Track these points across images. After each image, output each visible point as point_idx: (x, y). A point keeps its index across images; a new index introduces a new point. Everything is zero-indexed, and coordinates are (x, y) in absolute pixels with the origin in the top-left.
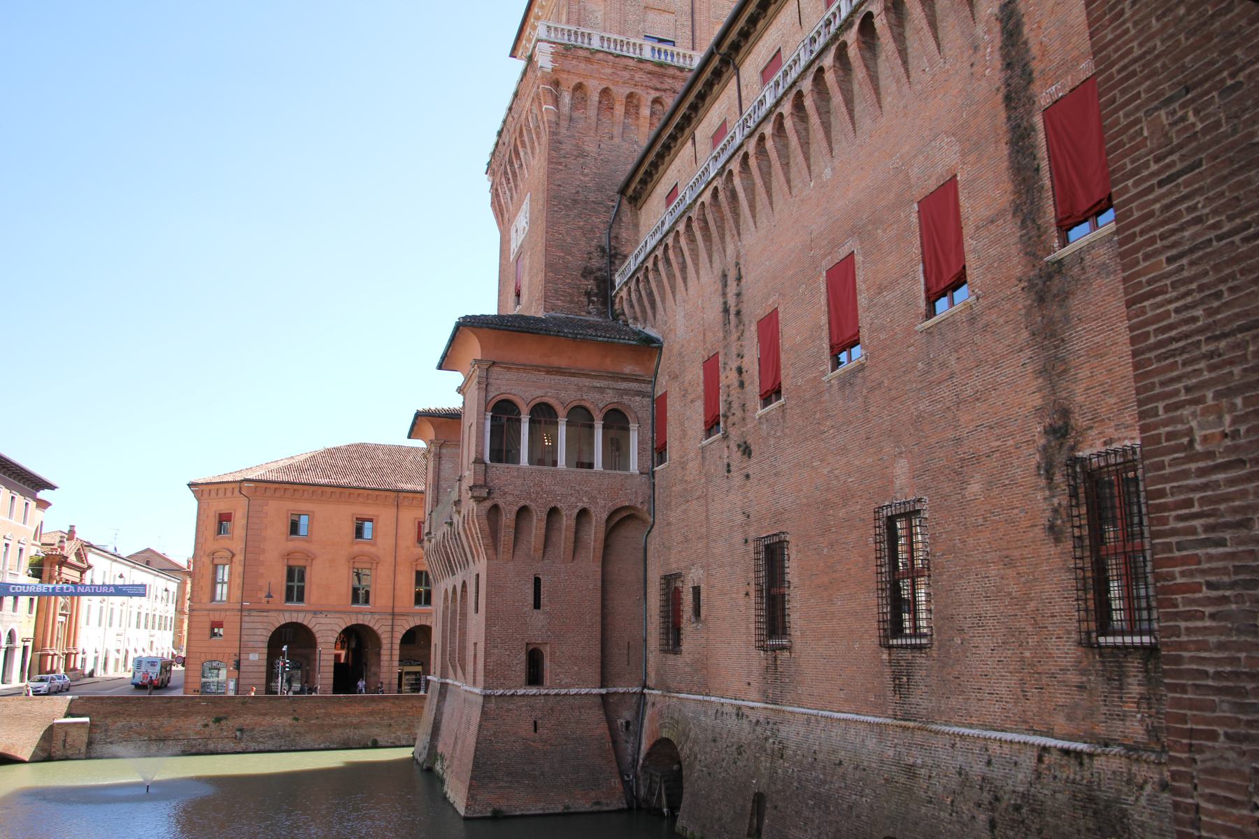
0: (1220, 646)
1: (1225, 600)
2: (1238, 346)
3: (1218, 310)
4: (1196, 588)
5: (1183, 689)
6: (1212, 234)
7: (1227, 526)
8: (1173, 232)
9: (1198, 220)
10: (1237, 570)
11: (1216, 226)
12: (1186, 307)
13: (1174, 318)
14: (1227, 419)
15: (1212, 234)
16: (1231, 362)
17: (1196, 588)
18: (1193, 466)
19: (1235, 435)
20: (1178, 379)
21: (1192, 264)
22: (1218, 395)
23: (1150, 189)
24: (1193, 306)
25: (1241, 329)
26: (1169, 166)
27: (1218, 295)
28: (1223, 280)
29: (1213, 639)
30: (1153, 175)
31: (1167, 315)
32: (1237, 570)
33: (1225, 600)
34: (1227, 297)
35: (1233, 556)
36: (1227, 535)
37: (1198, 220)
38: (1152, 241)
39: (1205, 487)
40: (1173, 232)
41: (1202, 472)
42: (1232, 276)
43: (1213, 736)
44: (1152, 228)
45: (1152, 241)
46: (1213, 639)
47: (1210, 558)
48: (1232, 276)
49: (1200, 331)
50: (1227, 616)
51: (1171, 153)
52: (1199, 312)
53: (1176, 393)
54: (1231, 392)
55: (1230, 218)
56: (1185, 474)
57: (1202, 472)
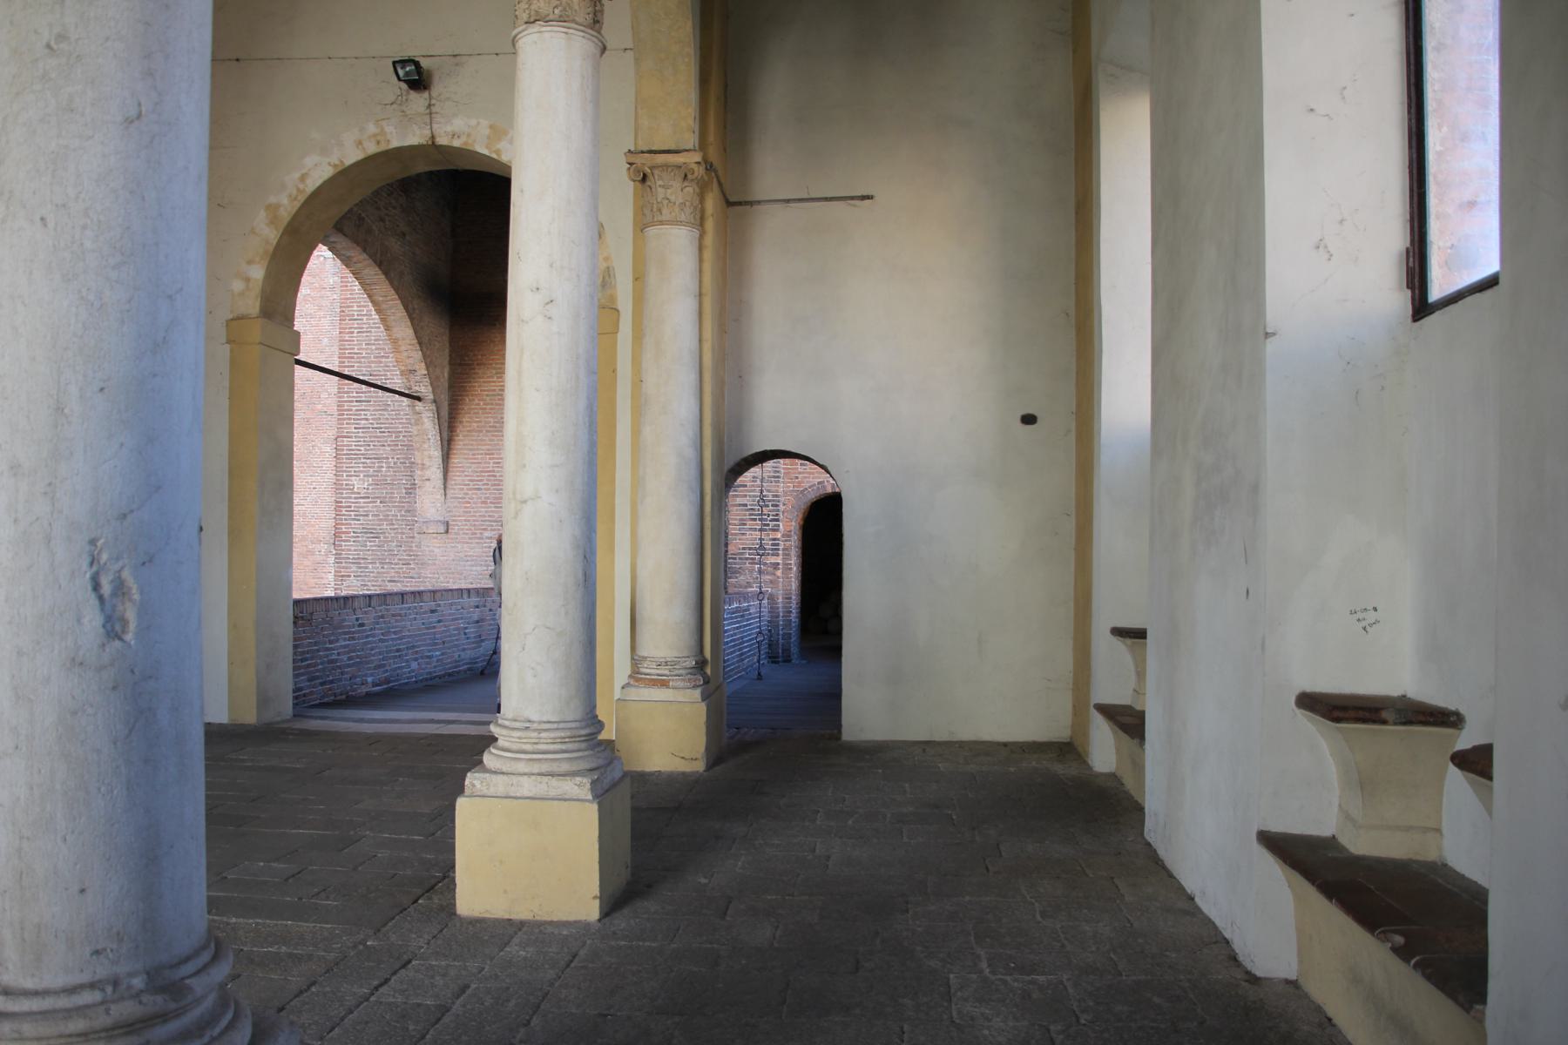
0: (355, 550)
1: (358, 537)
2: (372, 463)
3: (368, 450)
4: (349, 533)
5: (341, 563)
6: (370, 426)
7: (362, 515)
8: (358, 419)
9: (367, 419)
10: (363, 528)
11: (372, 424)
12: (358, 446)
13: (354, 447)
14: (366, 484)
15: (370, 426)
16: (370, 467)
17: (349, 533)
18: (353, 496)
19: (368, 489)
20: (352, 467)
21: (363, 432)
22: (364, 476)
23: (352, 401)
24: (361, 446)
25: (375, 458)
26: (359, 397)
27: (369, 445)
28: (372, 442)
29: (353, 548)
30: (354, 397)
31: (351, 446)
32: (363, 528)
33: (358, 537)
34: (372, 447)
35: (362, 524)
36: (361, 518)
37: (367, 419)
38: (350, 419)
39: (357, 503)
40: (358, 419)
41: (355, 498)
42: (375, 441)
43: (349, 576)
44: (351, 415)
45: (350, 419)
46: (353, 548)
47: (355, 524)
48: (375, 441)
49: (362, 455)
50: (358, 541)
51: (362, 393)
52: (362, 448)
53: (350, 471)
54: (368, 476)
55: (377, 424)
56: (350, 498)
57: (355, 498)
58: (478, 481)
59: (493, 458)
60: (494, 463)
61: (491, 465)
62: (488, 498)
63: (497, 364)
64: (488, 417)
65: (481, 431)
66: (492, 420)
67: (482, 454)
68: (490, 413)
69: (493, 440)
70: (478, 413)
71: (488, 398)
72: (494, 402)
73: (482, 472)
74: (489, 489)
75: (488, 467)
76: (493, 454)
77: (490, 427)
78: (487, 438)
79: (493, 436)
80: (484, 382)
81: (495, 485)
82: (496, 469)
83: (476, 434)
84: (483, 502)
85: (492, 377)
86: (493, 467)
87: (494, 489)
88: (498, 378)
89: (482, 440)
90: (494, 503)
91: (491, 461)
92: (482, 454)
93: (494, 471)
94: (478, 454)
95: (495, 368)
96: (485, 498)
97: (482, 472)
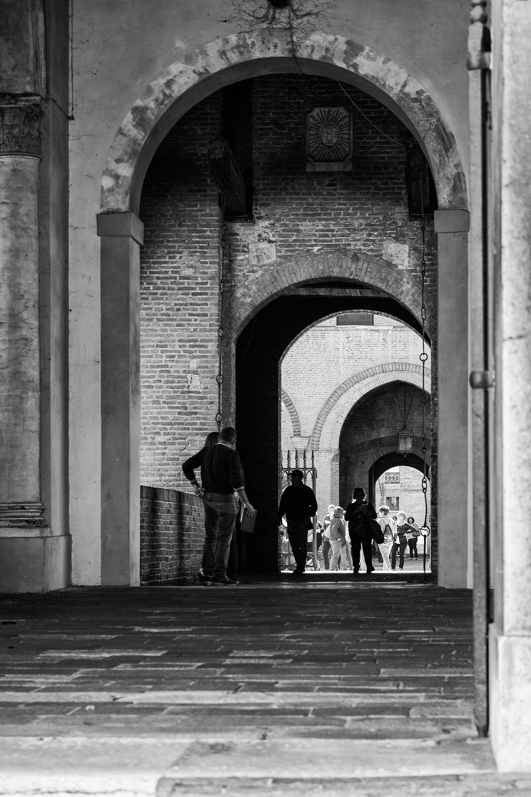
58: (149, 377)
59: (166, 351)
60: (167, 357)
61: (164, 358)
62: (161, 397)
63: (168, 241)
64: (159, 304)
65: (151, 320)
66: (164, 307)
67: (153, 346)
68: (162, 299)
69: (166, 330)
70: (147, 299)
71: (159, 282)
72: (166, 286)
73: (152, 367)
74: (160, 387)
75: (161, 361)
76: (166, 346)
77: (162, 315)
78: (159, 328)
79: (166, 325)
80: (153, 263)
81: (168, 382)
82: (170, 364)
83: (146, 323)
84: (154, 402)
85: (164, 257)
86: (166, 361)
87: (167, 387)
88: (170, 258)
89: (153, 330)
90: (168, 403)
91: (164, 355)
92: (153, 346)
93: (167, 366)
94: (149, 346)
95: (167, 247)
96: (157, 397)
97: (152, 367)
